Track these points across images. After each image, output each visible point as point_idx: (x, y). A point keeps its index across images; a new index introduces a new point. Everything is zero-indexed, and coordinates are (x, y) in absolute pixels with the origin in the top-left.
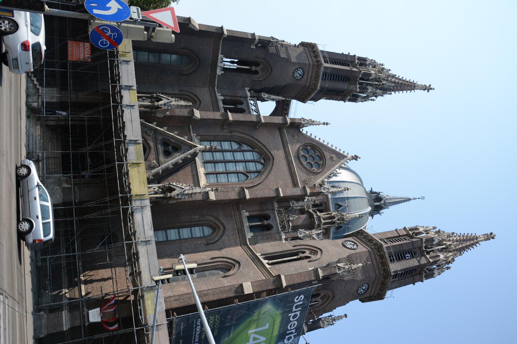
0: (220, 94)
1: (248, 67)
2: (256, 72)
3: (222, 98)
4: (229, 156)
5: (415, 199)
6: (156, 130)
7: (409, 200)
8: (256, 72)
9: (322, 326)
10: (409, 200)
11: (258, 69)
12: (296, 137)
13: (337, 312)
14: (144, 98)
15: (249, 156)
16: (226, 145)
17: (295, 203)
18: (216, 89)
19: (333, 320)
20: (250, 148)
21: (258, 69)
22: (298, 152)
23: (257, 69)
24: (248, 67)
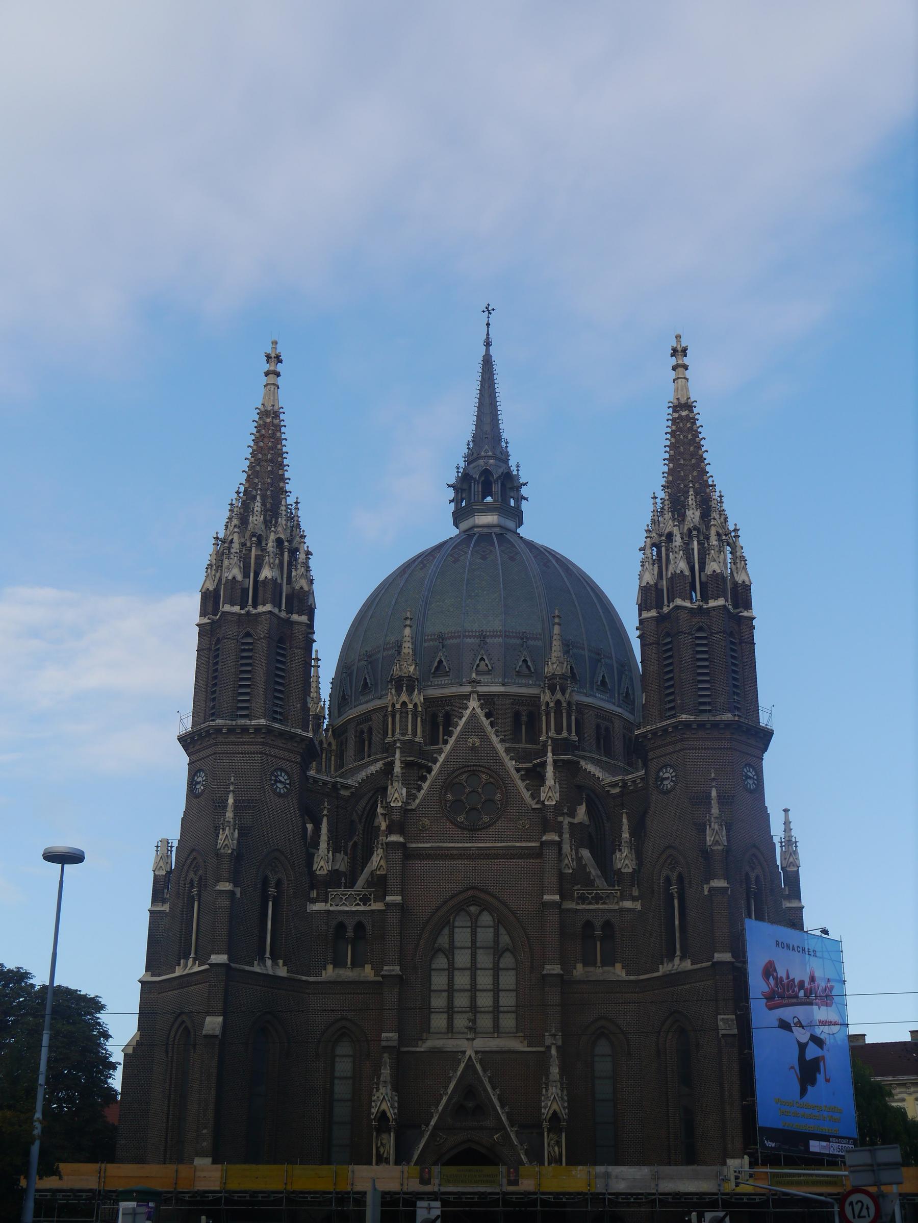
0: (324, 972)
1: (270, 904)
2: (279, 883)
3: (330, 968)
4: (462, 980)
5: (488, 344)
6: (436, 1127)
7: (487, 364)
8: (279, 883)
9: (795, 869)
10: (487, 364)
11: (273, 881)
12: (427, 822)
13: (777, 831)
14: (379, 1145)
15: (462, 936)
16: (439, 981)
17: (566, 861)
18: (311, 979)
19: (789, 843)
20: (446, 931)
21: (273, 881)
22: (460, 826)
23: (273, 883)
24: (270, 904)
